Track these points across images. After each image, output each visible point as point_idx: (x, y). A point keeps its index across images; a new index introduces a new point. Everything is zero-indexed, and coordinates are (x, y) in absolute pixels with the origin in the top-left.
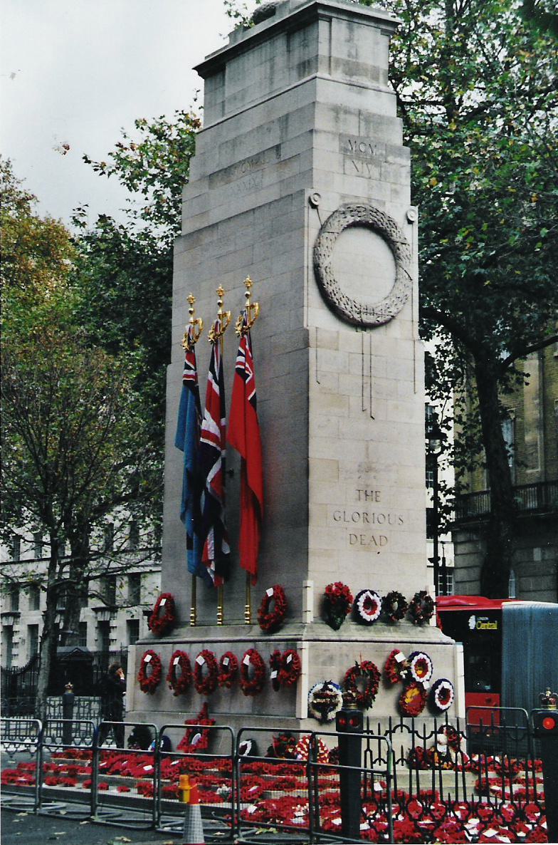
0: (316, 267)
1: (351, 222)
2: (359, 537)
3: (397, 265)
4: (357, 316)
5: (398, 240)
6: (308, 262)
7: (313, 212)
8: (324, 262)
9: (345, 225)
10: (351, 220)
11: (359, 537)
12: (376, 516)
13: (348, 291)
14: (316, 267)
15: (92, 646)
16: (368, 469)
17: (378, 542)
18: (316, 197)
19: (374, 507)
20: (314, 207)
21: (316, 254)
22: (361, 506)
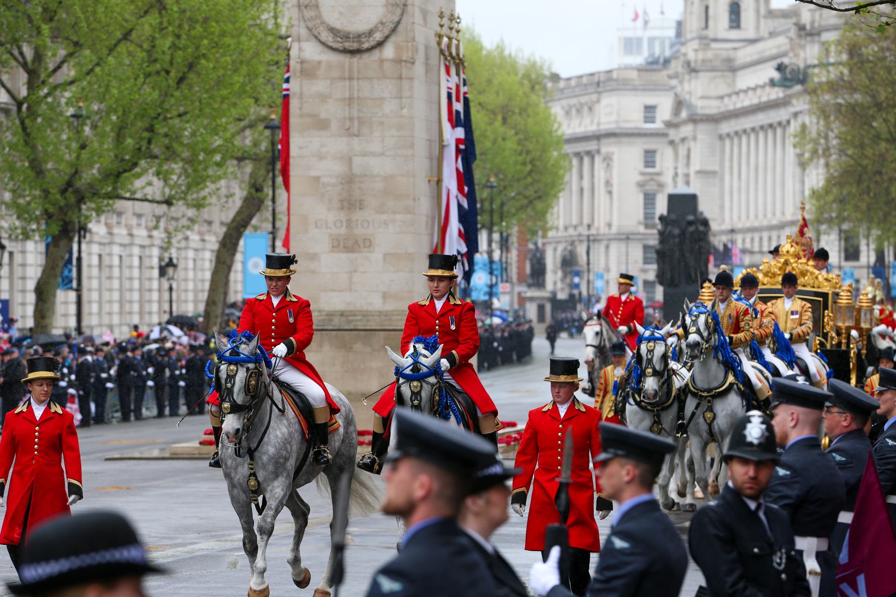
12: (359, 222)
17: (361, 244)
19: (358, 215)
22: (342, 216)
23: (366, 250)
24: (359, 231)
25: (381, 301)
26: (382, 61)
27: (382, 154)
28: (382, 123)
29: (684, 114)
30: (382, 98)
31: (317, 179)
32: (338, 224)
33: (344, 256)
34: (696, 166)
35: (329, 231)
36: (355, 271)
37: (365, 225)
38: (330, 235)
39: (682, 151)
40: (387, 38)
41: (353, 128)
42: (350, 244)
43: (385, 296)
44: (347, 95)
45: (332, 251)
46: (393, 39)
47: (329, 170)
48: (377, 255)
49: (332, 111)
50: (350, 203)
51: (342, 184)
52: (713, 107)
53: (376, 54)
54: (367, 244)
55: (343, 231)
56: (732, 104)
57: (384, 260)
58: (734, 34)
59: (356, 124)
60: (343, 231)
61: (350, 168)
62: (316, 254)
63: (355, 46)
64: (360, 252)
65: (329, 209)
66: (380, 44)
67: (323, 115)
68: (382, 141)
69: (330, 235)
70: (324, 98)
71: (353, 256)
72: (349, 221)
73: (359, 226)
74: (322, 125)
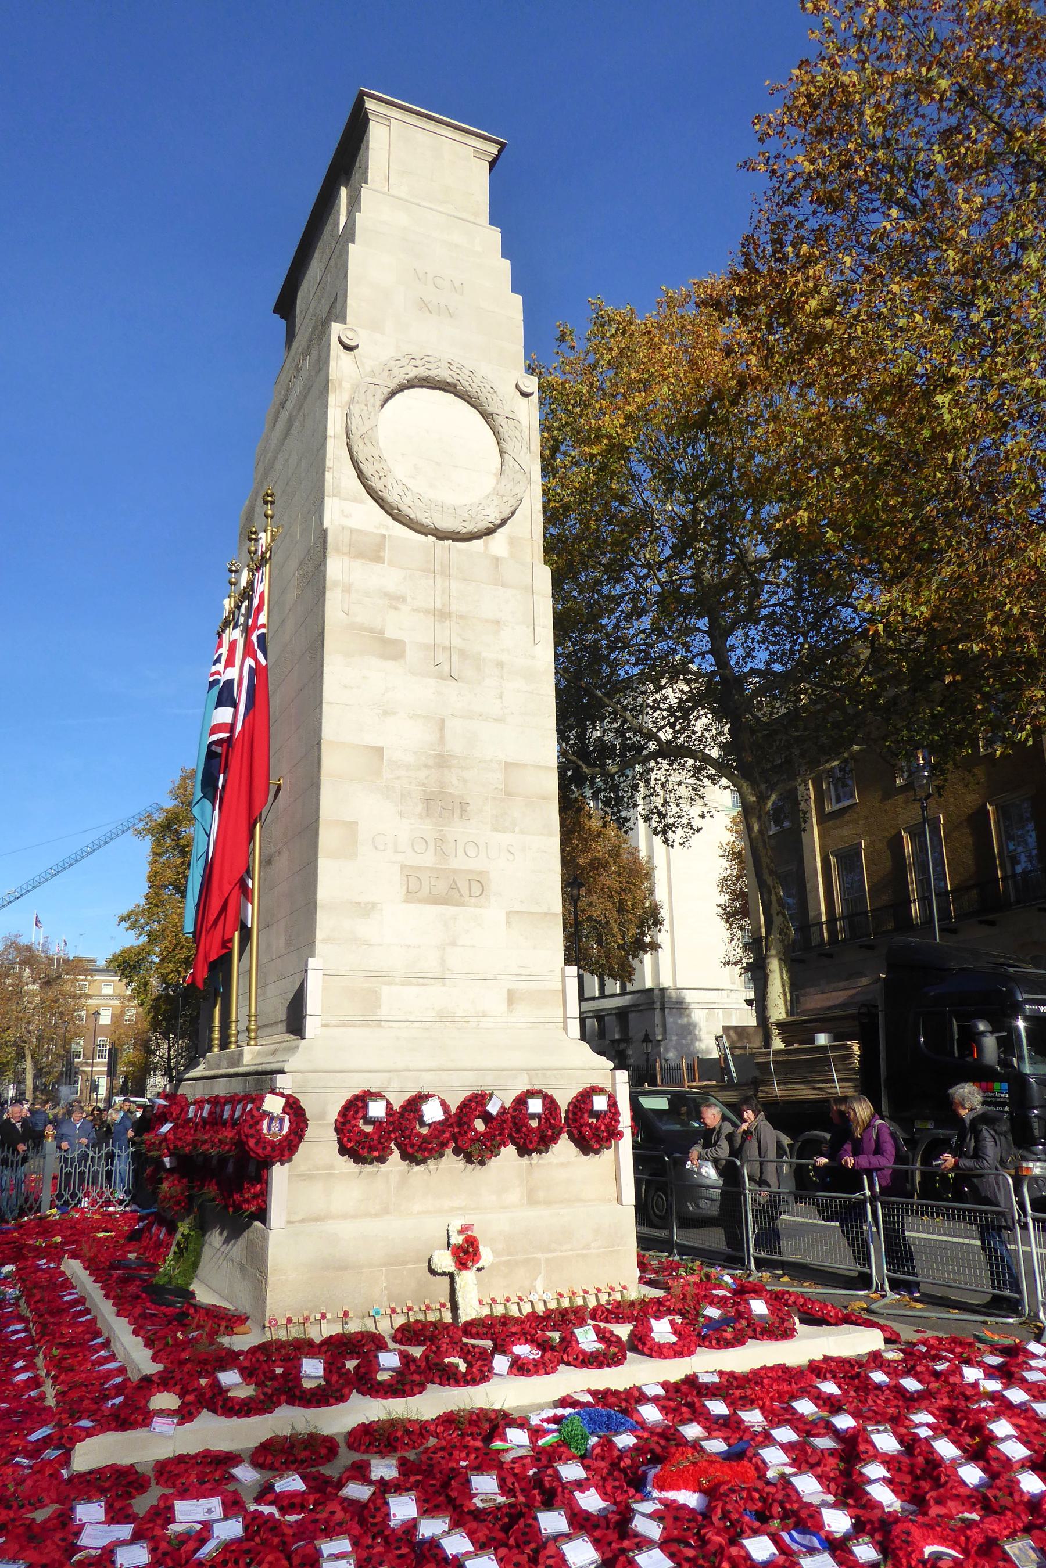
1: (411, 375)
16: (442, 761)
17: (465, 891)
23: (473, 900)
24: (457, 862)
25: (503, 1007)
28: (500, 665)
30: (498, 622)
31: (379, 751)
33: (433, 911)
36: (453, 944)
37: (472, 852)
38: (403, 867)
43: (512, 998)
45: (406, 901)
47: (405, 739)
50: (441, 804)
51: (426, 766)
55: (428, 859)
59: (455, 658)
61: (442, 738)
62: (374, 905)
64: (463, 904)
65: (401, 814)
66: (490, 532)
67: (390, 633)
69: (403, 867)
70: (395, 600)
71: (451, 910)
72: (440, 840)
73: (460, 852)
74: (391, 649)
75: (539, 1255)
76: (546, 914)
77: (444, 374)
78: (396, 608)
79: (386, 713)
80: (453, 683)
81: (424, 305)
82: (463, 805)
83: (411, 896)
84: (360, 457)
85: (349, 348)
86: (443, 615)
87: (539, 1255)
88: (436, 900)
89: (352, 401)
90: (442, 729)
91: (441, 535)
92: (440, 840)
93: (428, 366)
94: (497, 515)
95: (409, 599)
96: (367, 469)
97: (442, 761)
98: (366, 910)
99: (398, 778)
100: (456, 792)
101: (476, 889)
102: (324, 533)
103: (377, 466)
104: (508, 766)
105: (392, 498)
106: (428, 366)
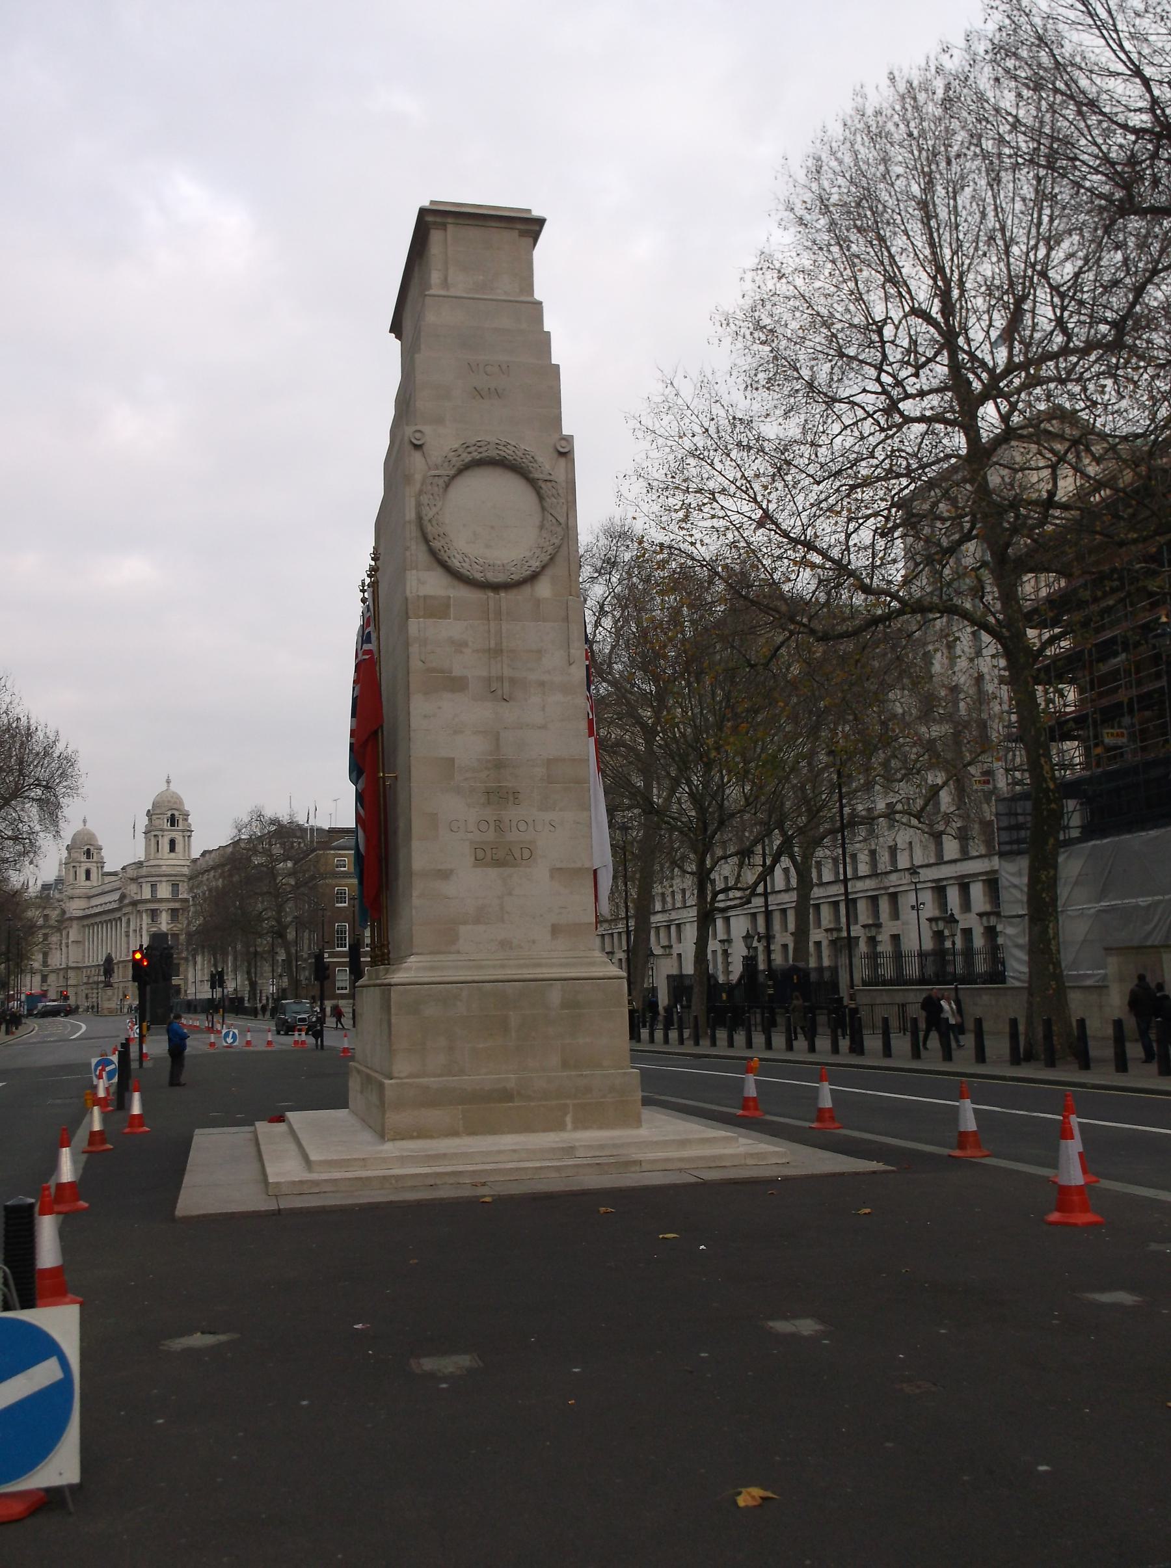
0: (420, 518)
1: (467, 460)
2: (489, 852)
3: (543, 509)
4: (478, 576)
5: (541, 476)
6: (411, 515)
7: (417, 456)
8: (428, 513)
9: (459, 464)
10: (467, 458)
11: (489, 852)
12: (514, 824)
13: (465, 547)
14: (420, 518)
15: (813, 963)
17: (517, 855)
18: (418, 435)
20: (418, 447)
21: (419, 505)
26: (538, 602)
27: (544, 727)
28: (542, 684)
29: (126, 901)
30: (539, 651)
31: (452, 760)
32: (484, 827)
33: (493, 873)
34: (71, 939)
35: (470, 836)
36: (510, 894)
37: (522, 827)
39: (64, 933)
40: (544, 567)
41: (500, 690)
42: (499, 854)
43: (556, 930)
44: (493, 645)
45: (475, 866)
46: (549, 572)
47: (468, 749)
48: (541, 871)
49: (468, 665)
50: (499, 796)
52: (80, 913)
53: (526, 590)
54: (526, 854)
55: (491, 835)
56: (88, 912)
57: (552, 877)
58: (88, 883)
59: (506, 684)
60: (491, 835)
62: (452, 871)
63: (500, 578)
66: (533, 577)
67: (457, 672)
68: (543, 710)
70: (459, 646)
71: (508, 871)
72: (498, 821)
74: (457, 685)
75: (568, 1101)
76: (580, 869)
77: (493, 453)
78: (461, 652)
79: (455, 732)
80: (504, 703)
81: (478, 393)
82: (516, 793)
83: (479, 862)
84: (430, 537)
85: (418, 447)
86: (495, 652)
87: (568, 1101)
88: (498, 863)
89: (421, 492)
90: (498, 740)
91: (496, 587)
92: (498, 821)
93: (480, 450)
94: (538, 564)
95: (470, 644)
96: (436, 544)
97: (499, 765)
98: (445, 875)
99: (466, 779)
100: (510, 785)
101: (526, 854)
102: (406, 599)
103: (443, 542)
104: (550, 763)
105: (455, 563)
106: (480, 450)
